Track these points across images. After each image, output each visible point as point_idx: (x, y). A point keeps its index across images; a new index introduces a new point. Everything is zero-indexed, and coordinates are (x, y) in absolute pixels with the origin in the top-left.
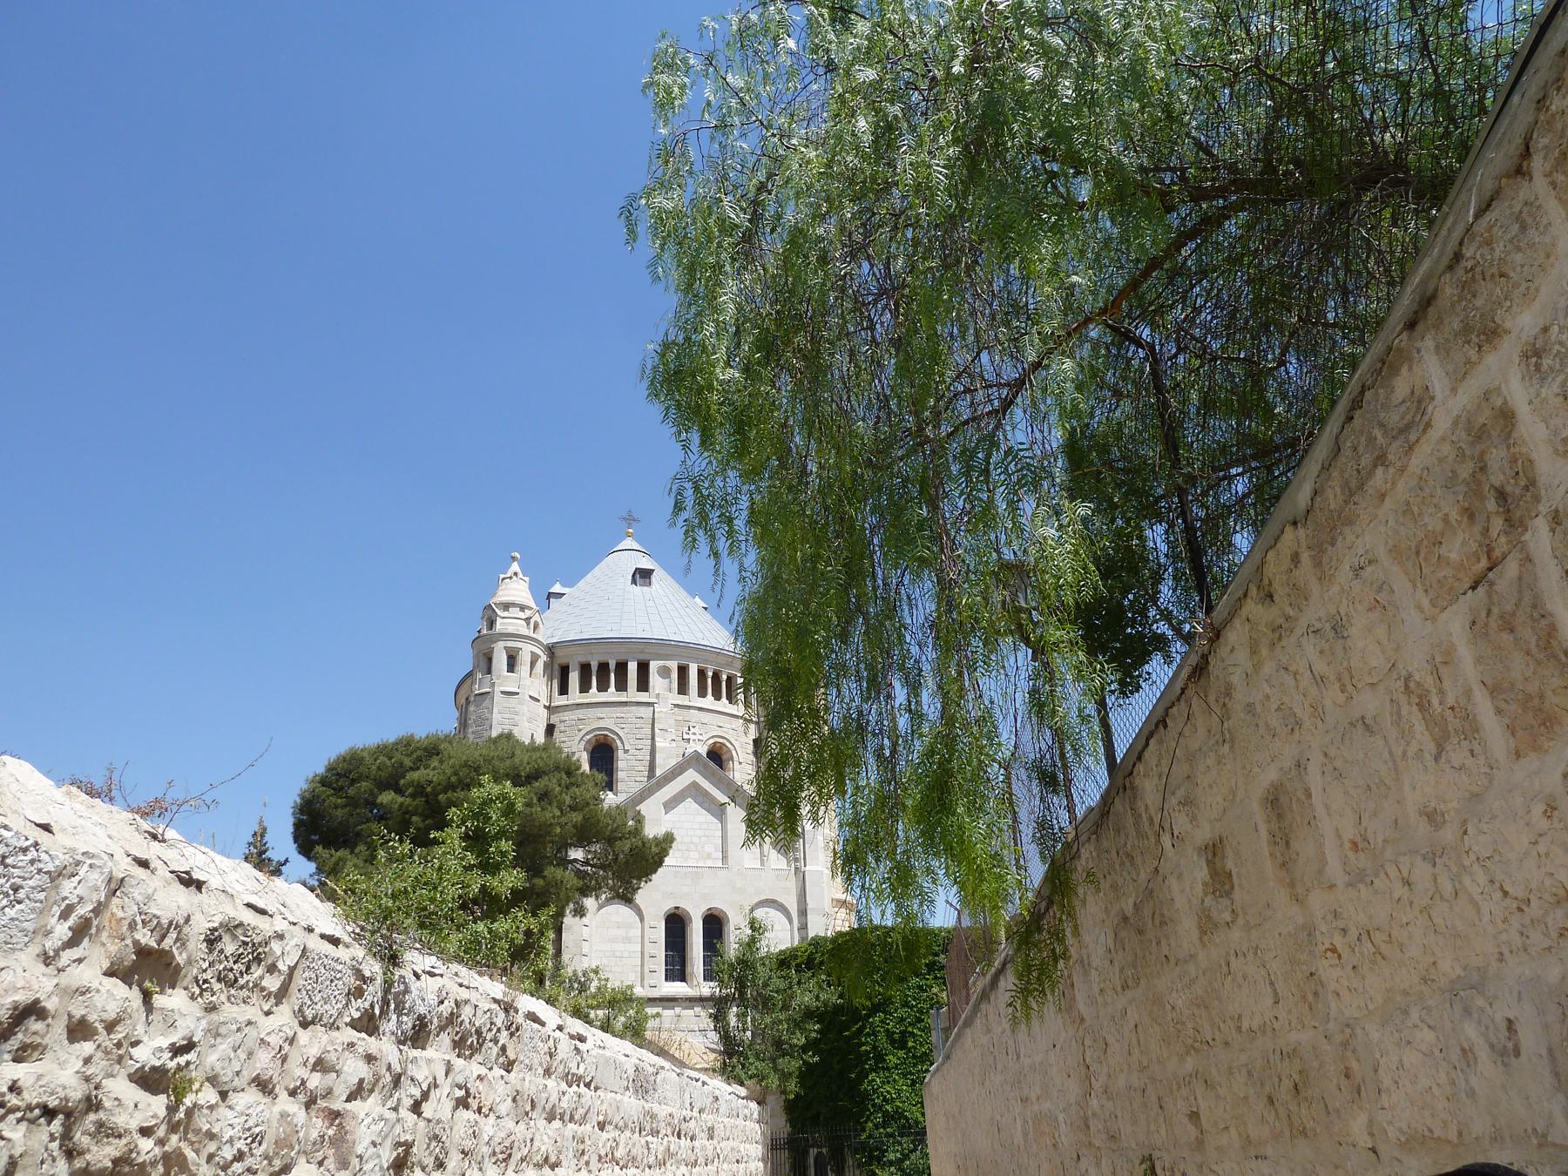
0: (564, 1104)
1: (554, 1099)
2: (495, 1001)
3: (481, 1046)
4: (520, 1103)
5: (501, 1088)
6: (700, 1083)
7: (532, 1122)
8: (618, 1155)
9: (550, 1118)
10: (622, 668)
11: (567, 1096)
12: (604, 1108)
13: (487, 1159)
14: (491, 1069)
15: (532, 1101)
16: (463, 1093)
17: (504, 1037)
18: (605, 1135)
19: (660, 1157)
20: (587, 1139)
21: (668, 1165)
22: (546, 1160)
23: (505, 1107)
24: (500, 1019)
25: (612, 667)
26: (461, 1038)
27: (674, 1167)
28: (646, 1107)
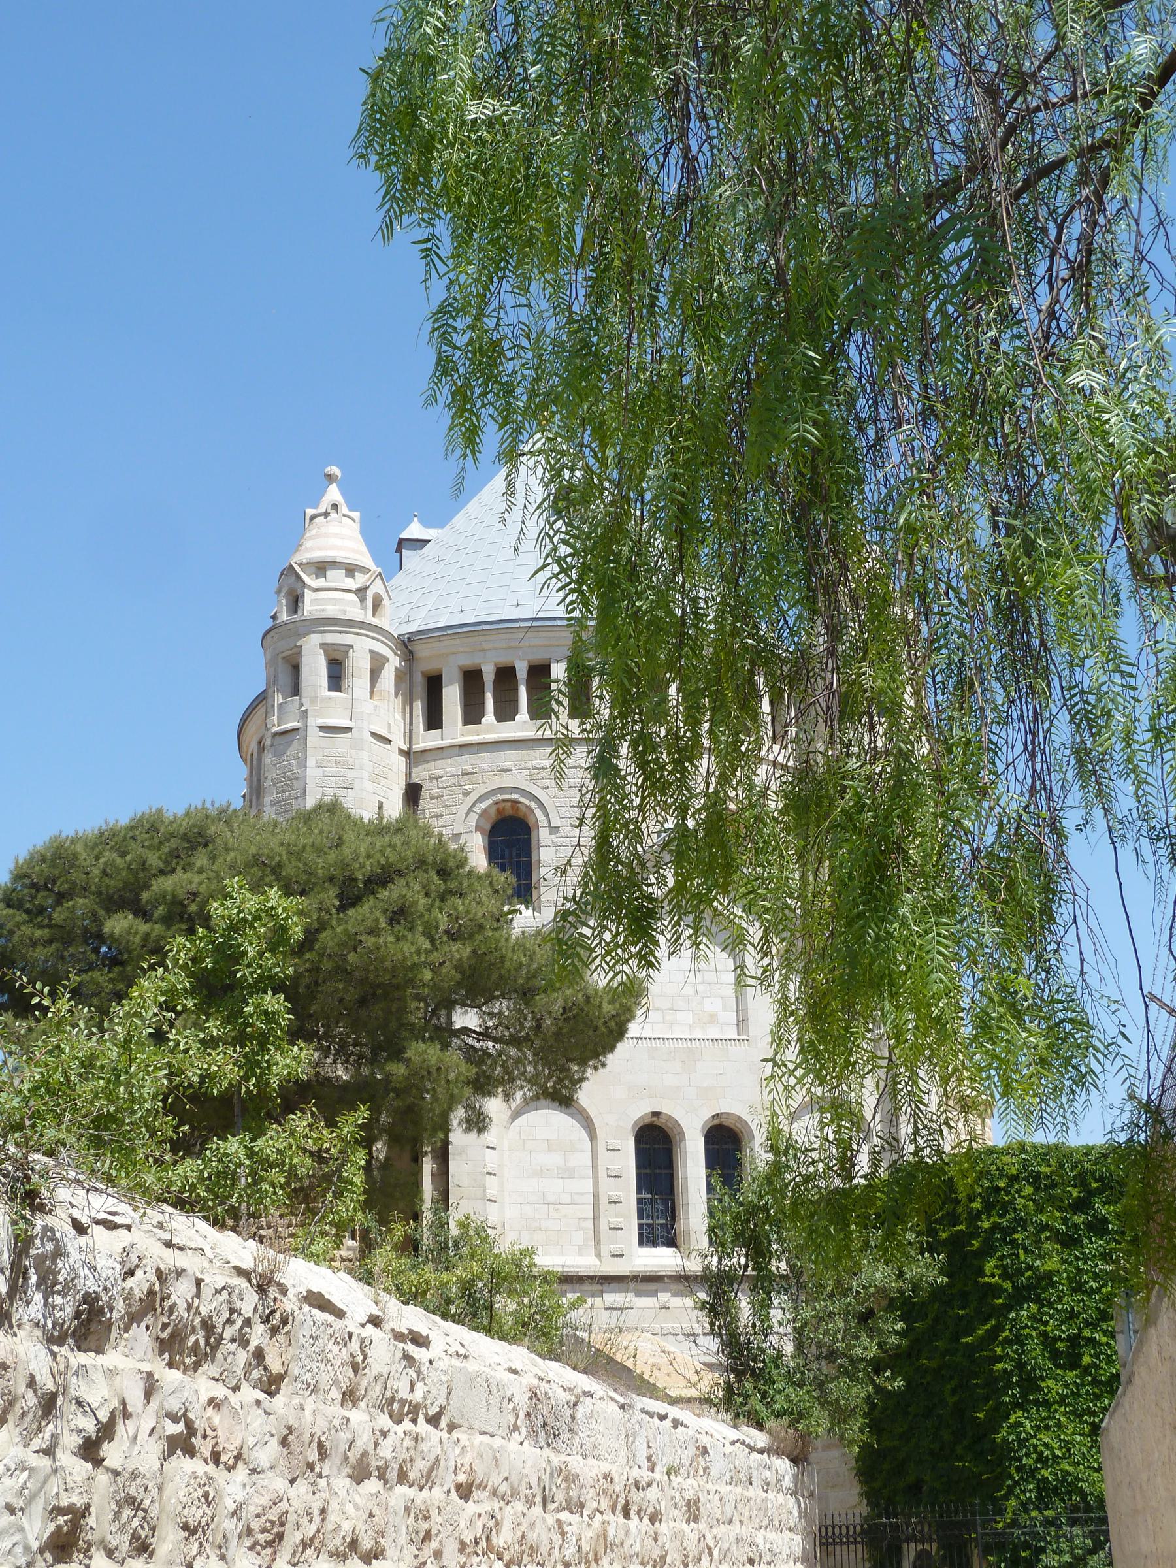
0: (386, 1451)
1: (364, 1441)
2: (240, 1272)
3: (214, 1349)
4: (297, 1449)
5: (256, 1419)
6: (668, 1423)
7: (322, 1483)
8: (500, 1541)
9: (360, 1474)
10: (539, 673)
11: (391, 1438)
12: (467, 1460)
13: (234, 1541)
14: (236, 1388)
15: (321, 1445)
16: (180, 1427)
17: (258, 1334)
18: (471, 1508)
19: (586, 1547)
20: (434, 1513)
22: (354, 1545)
24: (249, 1303)
25: (522, 673)
26: (172, 1336)
28: (557, 1460)
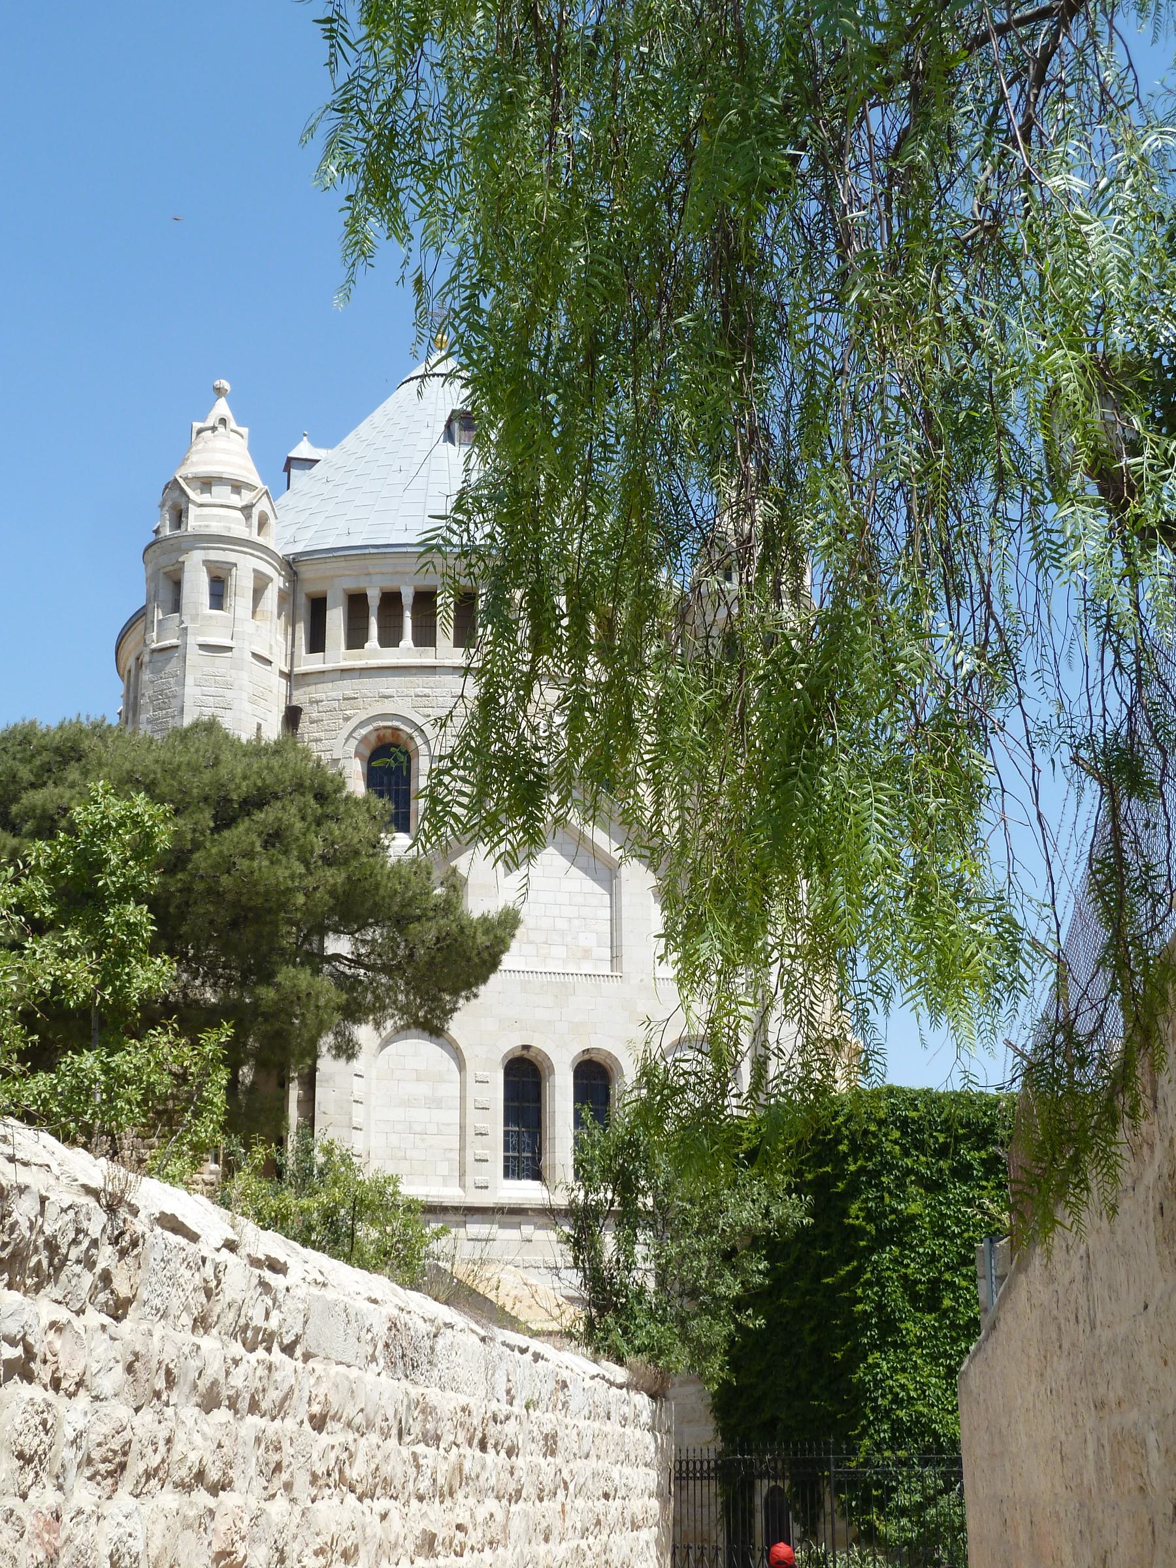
0: (237, 1379)
1: (214, 1369)
2: (88, 1190)
3: (58, 1270)
4: (142, 1376)
5: (101, 1347)
6: (528, 1357)
7: (169, 1411)
8: (352, 1473)
9: (209, 1403)
10: (425, 600)
11: (243, 1366)
12: (321, 1391)
13: (72, 1471)
14: (80, 1312)
15: (168, 1372)
16: (19, 1351)
17: (106, 1256)
18: (324, 1439)
19: (441, 1481)
20: (286, 1444)
21: (460, 1495)
22: (200, 1476)
23: (111, 1381)
24: (97, 1223)
25: (407, 599)
26: (13, 1255)
27: (472, 1501)
28: (415, 1392)
